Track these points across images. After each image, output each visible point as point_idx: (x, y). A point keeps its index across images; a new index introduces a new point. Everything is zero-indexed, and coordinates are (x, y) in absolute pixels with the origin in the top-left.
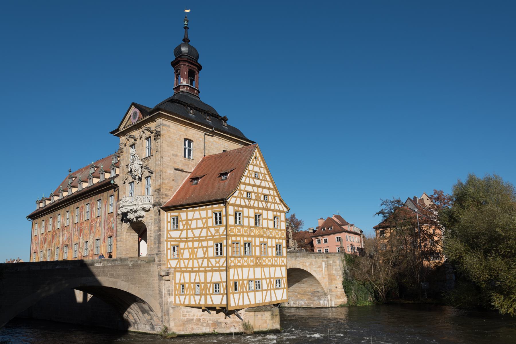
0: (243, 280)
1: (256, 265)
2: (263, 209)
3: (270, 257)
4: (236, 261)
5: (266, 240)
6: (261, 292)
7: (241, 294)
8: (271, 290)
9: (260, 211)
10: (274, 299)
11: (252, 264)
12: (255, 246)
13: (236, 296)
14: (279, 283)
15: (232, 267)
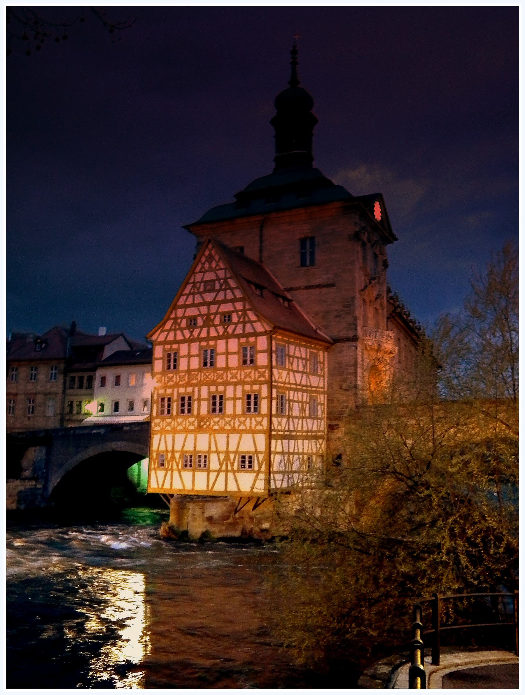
0: (173, 451)
1: (200, 429)
2: (219, 337)
3: (229, 416)
4: (163, 424)
5: (221, 388)
6: (205, 474)
7: (169, 472)
8: (227, 471)
9: (212, 343)
10: (232, 487)
11: (191, 427)
12: (199, 400)
13: (161, 473)
14: (250, 462)
15: (157, 432)
